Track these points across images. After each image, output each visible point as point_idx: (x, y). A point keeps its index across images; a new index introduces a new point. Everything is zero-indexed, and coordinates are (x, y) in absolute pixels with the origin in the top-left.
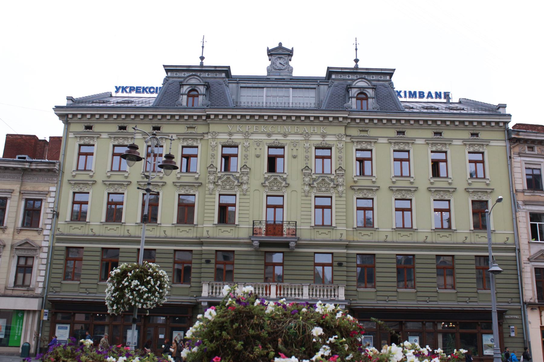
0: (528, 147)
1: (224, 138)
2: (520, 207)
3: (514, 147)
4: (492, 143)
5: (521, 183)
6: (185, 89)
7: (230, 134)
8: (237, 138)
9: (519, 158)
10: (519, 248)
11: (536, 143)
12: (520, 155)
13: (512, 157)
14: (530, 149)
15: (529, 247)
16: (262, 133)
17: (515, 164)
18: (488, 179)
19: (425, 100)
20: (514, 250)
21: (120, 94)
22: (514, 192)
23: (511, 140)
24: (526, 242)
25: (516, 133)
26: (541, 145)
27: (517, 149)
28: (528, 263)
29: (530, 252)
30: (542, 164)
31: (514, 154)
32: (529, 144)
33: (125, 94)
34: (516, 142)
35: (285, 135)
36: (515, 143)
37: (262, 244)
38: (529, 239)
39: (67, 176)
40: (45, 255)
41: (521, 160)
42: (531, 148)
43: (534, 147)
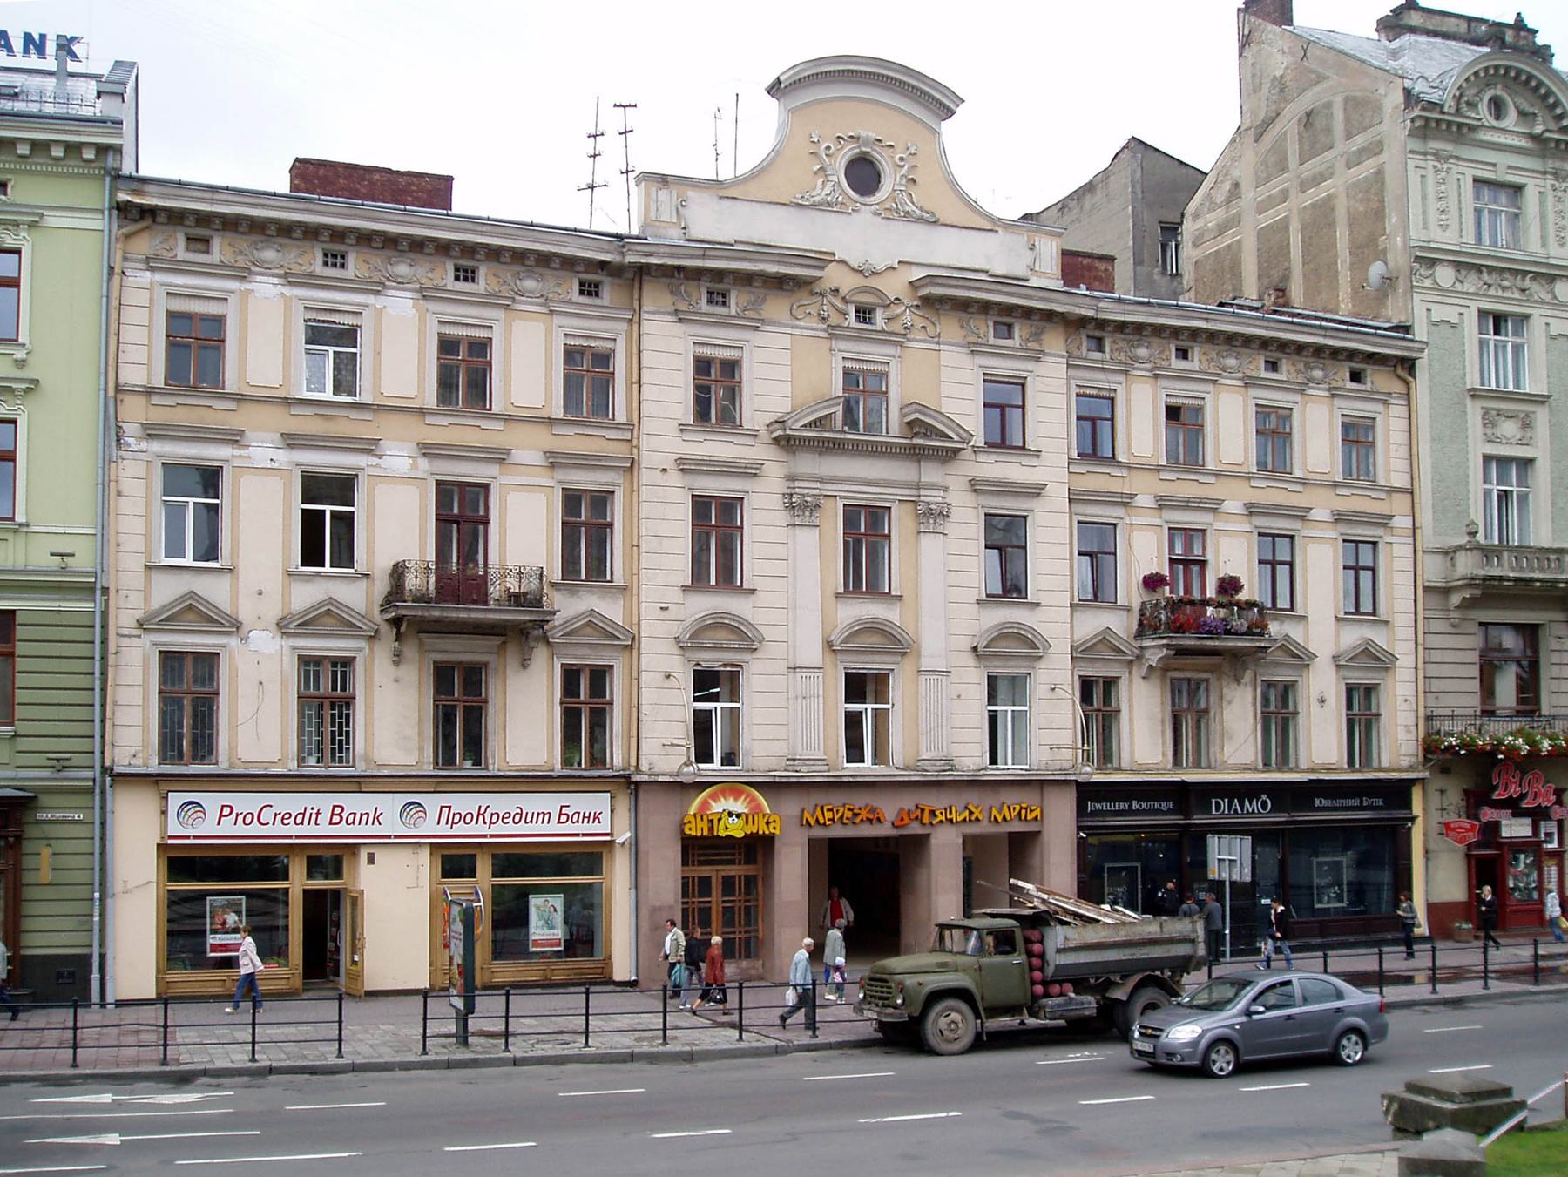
0: (190, 239)
2: (129, 445)
3: (127, 237)
9: (148, 273)
10: (105, 586)
11: (216, 227)
12: (151, 264)
13: (117, 270)
14: (199, 246)
15: (148, 581)
17: (130, 297)
18: (24, 345)
22: (111, 393)
23: (123, 209)
24: (137, 563)
25: (135, 185)
26: (236, 231)
27: (144, 244)
28: (135, 636)
29: (147, 599)
30: (232, 299)
31: (125, 259)
32: (190, 227)
34: (142, 218)
36: (136, 221)
38: (148, 552)
41: (151, 284)
42: (199, 243)
43: (212, 237)
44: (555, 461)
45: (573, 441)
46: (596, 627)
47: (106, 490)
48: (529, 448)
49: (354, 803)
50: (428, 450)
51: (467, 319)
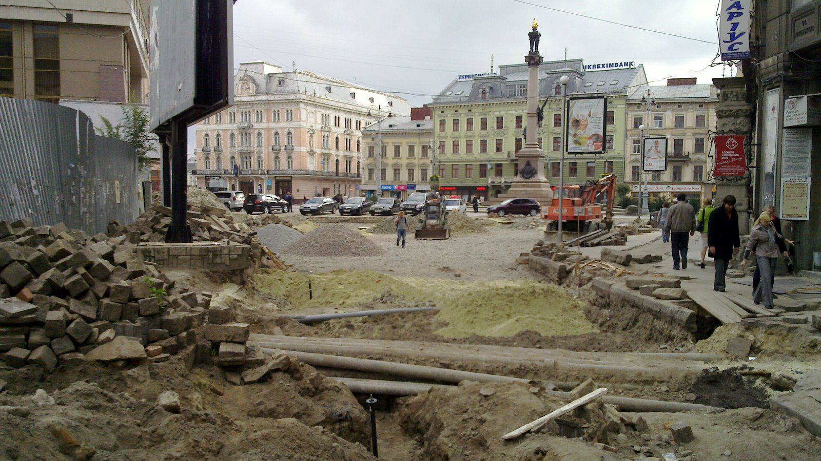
1: (497, 114)
4: (618, 106)
5: (631, 125)
6: (481, 90)
7: (500, 111)
8: (503, 113)
16: (513, 110)
19: (619, 67)
20: (622, 158)
21: (461, 80)
27: (631, 108)
33: (463, 80)
35: (523, 111)
37: (513, 160)
39: (436, 135)
40: (431, 168)
44: (693, 134)
45: (698, 131)
46: (699, 160)
47: (625, 144)
48: (689, 133)
49: (659, 186)
50: (672, 135)
51: (680, 113)
